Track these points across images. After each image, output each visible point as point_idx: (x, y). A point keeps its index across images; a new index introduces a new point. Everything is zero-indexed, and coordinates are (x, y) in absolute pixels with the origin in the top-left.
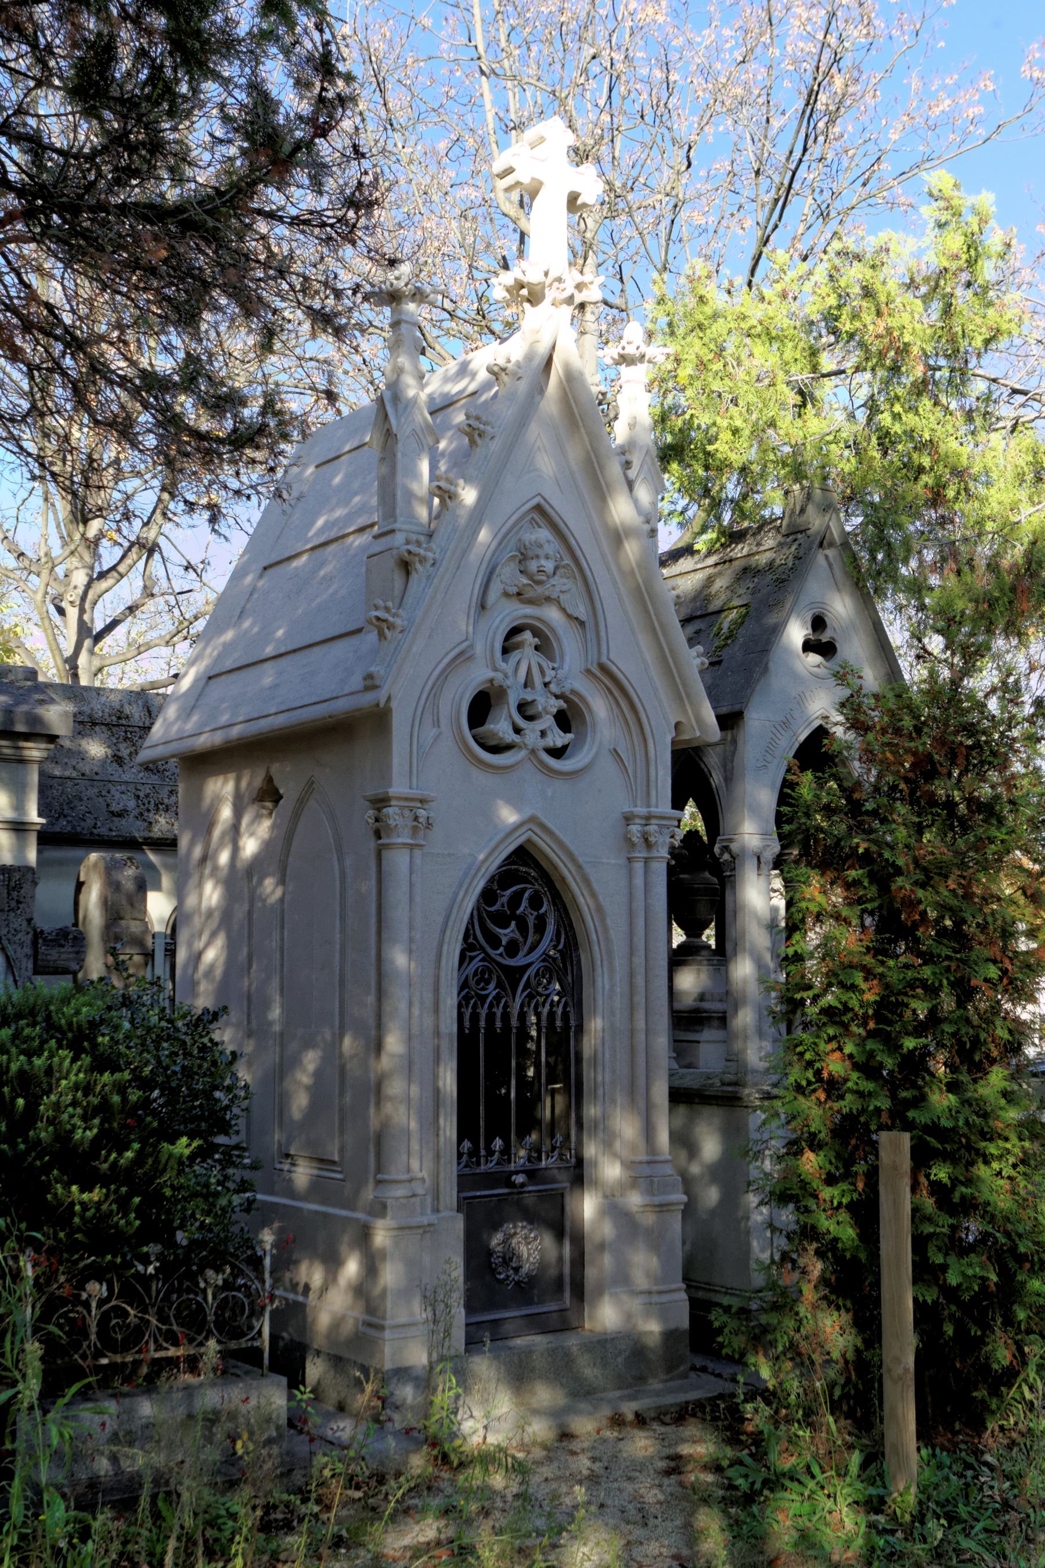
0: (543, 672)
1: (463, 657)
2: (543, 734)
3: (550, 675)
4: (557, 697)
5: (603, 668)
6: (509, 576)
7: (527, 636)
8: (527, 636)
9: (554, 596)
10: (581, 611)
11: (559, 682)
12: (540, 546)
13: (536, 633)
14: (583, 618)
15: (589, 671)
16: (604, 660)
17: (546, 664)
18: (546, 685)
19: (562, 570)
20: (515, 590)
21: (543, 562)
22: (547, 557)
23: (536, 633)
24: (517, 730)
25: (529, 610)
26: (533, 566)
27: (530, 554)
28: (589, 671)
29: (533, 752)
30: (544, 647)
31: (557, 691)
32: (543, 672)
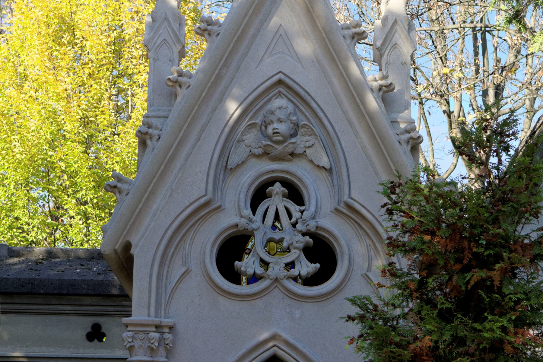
0: (290, 216)
1: (205, 210)
2: (291, 265)
3: (296, 215)
4: (304, 235)
5: (349, 207)
6: (252, 138)
7: (278, 188)
8: (278, 188)
9: (299, 151)
10: (324, 161)
11: (304, 222)
12: (272, 113)
13: (285, 183)
14: (328, 166)
15: (337, 210)
16: (346, 198)
17: (294, 208)
18: (294, 225)
19: (301, 131)
20: (260, 151)
21: (275, 125)
22: (280, 121)
23: (285, 183)
24: (265, 264)
25: (275, 166)
26: (270, 130)
27: (267, 121)
28: (331, 211)
29: (276, 280)
30: (295, 194)
31: (304, 229)
32: (290, 216)
